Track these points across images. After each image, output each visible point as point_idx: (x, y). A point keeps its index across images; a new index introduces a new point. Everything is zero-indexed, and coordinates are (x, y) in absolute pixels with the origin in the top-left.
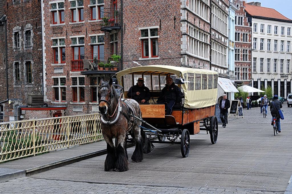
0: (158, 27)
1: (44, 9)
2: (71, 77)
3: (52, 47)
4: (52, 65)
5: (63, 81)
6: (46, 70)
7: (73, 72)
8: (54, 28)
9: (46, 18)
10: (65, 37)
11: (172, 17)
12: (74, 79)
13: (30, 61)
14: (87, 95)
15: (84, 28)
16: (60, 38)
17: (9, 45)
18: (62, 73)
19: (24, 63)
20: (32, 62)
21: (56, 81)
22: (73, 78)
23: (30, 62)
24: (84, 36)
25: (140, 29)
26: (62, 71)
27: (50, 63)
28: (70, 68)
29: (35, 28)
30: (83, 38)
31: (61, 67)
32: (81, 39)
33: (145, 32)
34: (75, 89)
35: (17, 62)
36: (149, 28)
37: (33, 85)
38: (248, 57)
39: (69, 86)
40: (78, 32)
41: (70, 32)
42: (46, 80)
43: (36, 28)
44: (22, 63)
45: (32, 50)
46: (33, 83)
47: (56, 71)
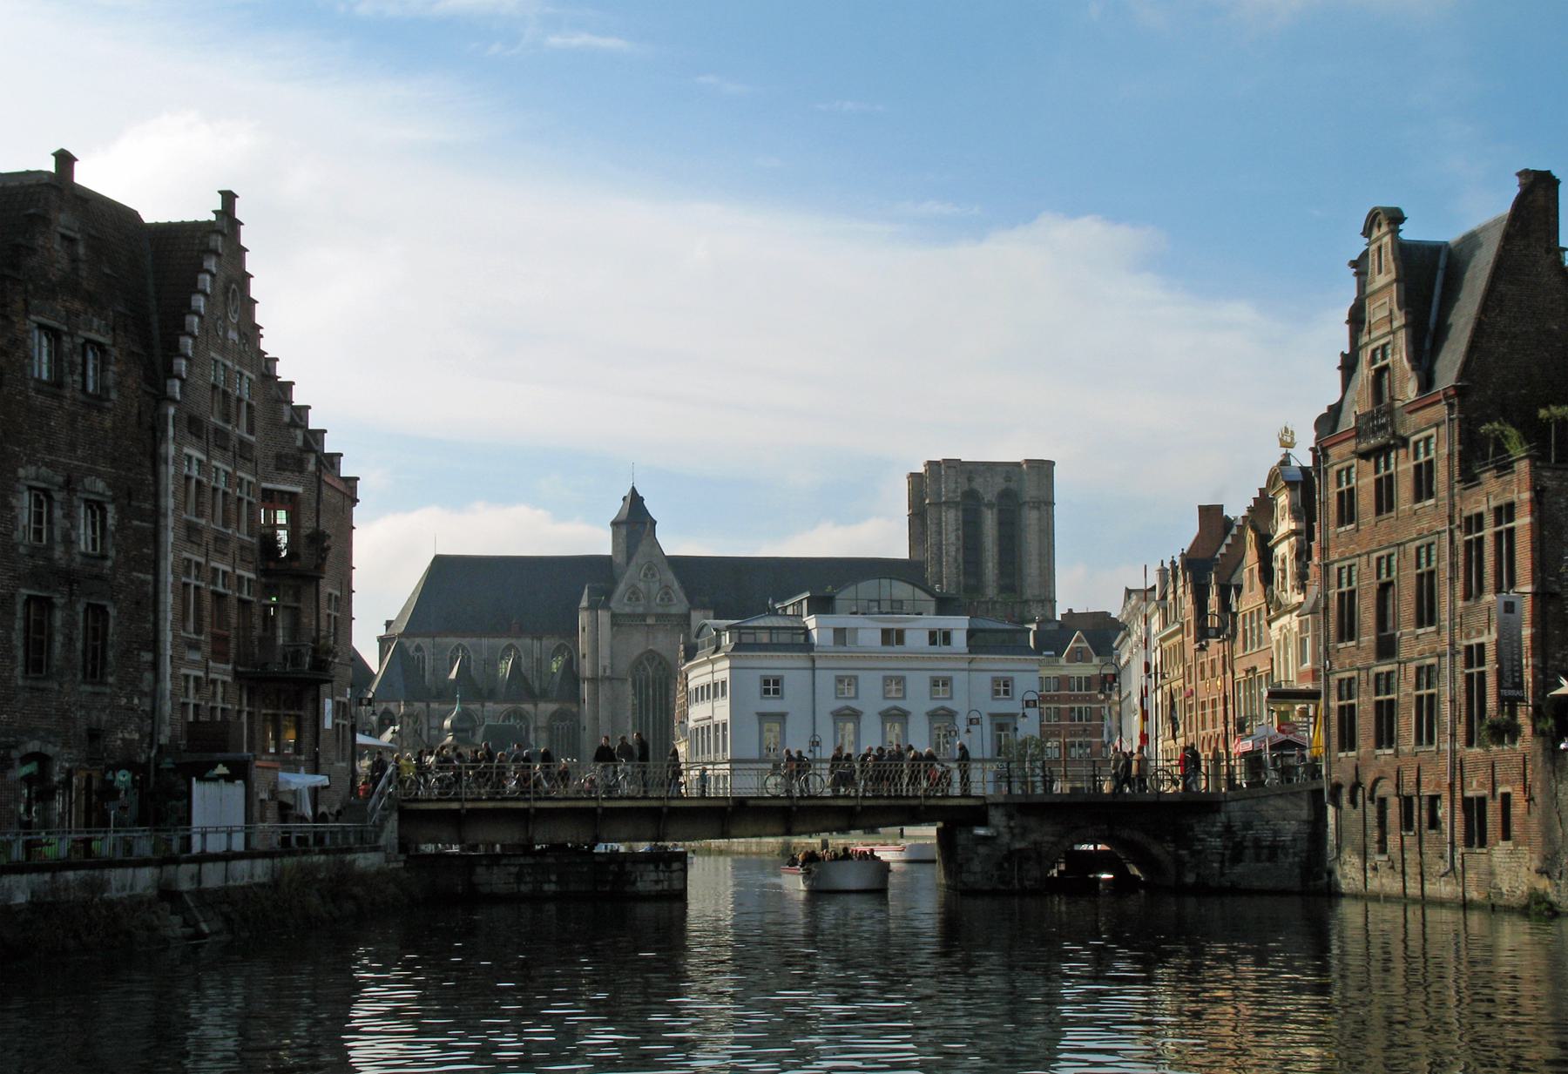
19: (80, 608)
20: (112, 611)
23: (103, 609)
29: (126, 502)
35: (45, 594)
43: (129, 505)
44: (70, 605)
45: (111, 568)
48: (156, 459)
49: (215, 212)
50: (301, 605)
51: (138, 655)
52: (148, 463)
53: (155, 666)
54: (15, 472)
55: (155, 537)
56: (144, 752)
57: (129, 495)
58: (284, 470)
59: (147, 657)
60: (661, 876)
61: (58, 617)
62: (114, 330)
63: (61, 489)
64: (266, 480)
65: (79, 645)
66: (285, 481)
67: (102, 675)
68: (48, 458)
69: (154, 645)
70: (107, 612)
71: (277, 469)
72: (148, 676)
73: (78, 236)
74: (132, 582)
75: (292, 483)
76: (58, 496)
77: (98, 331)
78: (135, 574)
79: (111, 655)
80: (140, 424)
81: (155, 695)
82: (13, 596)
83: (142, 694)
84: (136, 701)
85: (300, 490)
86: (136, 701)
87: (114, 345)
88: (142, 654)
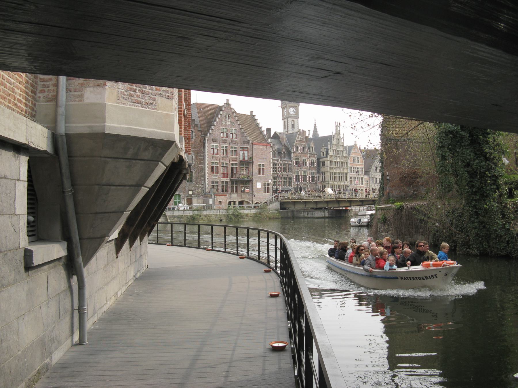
0: (264, 164)
4: (211, 174)
5: (217, 182)
6: (208, 176)
8: (213, 157)
10: (218, 162)
11: (268, 161)
12: (223, 182)
14: (230, 189)
15: (228, 159)
20: (194, 172)
21: (213, 182)
22: (222, 181)
26: (217, 177)
30: (227, 163)
31: (216, 176)
32: (226, 164)
34: (223, 187)
36: (261, 164)
38: (368, 185)
39: (220, 185)
41: (221, 160)
46: (194, 182)
47: (214, 177)
48: (204, 146)
49: (225, 103)
52: (202, 147)
53: (204, 180)
55: (204, 159)
57: (198, 153)
59: (202, 178)
60: (322, 214)
62: (194, 127)
64: (241, 146)
69: (204, 176)
72: (203, 181)
79: (194, 179)
81: (204, 184)
83: (201, 184)
84: (200, 185)
85: (248, 147)
86: (200, 185)
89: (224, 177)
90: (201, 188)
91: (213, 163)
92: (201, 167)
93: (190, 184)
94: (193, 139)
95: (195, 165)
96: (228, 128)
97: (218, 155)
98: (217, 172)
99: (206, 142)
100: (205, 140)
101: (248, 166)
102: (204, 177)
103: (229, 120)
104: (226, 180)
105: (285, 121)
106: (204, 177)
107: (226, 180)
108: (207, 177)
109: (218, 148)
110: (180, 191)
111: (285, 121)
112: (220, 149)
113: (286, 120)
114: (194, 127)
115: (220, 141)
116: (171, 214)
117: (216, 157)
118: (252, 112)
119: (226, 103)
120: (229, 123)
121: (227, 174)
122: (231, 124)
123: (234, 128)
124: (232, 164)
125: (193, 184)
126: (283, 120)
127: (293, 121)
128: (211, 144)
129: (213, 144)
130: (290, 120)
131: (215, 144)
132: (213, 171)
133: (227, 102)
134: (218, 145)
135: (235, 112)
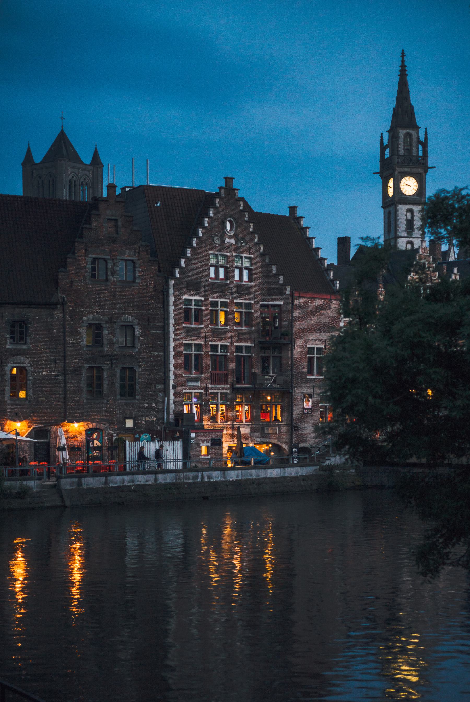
1: (174, 304)
2: (210, 391)
3: (184, 352)
6: (174, 381)
7: (213, 386)
9: (175, 315)
10: (202, 343)
13: (132, 366)
15: (229, 335)
16: (196, 342)
17: (70, 340)
18: (198, 386)
20: (138, 370)
24: (228, 344)
25: (308, 346)
26: (198, 384)
27: (180, 372)
28: (209, 380)
30: (226, 346)
33: (310, 350)
37: (138, 400)
40: (220, 339)
41: (210, 337)
42: (174, 394)
43: (148, 324)
46: (137, 397)
47: (190, 384)
49: (220, 188)
50: (282, 355)
51: (155, 386)
52: (160, 305)
54: (82, 318)
56: (160, 426)
58: (273, 295)
59: (160, 386)
61: (105, 375)
62: (139, 253)
63: (107, 322)
65: (118, 385)
66: (273, 300)
67: (135, 396)
68: (99, 311)
70: (135, 370)
71: (269, 295)
73: (118, 218)
74: (151, 356)
75: (278, 300)
76: (105, 326)
77: (129, 255)
78: (152, 353)
79: (138, 387)
80: (155, 290)
82: (80, 367)
83: (157, 402)
84: (154, 405)
85: (282, 303)
86: (154, 405)
87: (139, 259)
88: (157, 385)
89: (215, 381)
90: (157, 412)
91: (188, 346)
92: (158, 356)
93: (129, 401)
94: (134, 284)
95: (139, 352)
96: (228, 254)
97: (203, 326)
98: (199, 368)
99: (172, 291)
100: (168, 285)
101: (280, 353)
102: (164, 384)
103: (233, 233)
104: (223, 389)
105: (389, 212)
106: (164, 384)
107: (223, 389)
108: (172, 383)
109: (203, 308)
110: (103, 420)
111: (389, 212)
112: (207, 309)
113: (392, 209)
114: (139, 253)
115: (209, 290)
116: (72, 483)
117: (195, 330)
118: (293, 209)
119: (224, 186)
120: (233, 241)
121: (227, 375)
122: (236, 242)
123: (244, 253)
124: (239, 349)
125: (136, 401)
126: (384, 207)
127: (411, 211)
128: (184, 297)
129: (189, 297)
130: (402, 209)
131: (193, 298)
132: (187, 368)
133: (226, 185)
134: (203, 299)
135: (247, 207)
